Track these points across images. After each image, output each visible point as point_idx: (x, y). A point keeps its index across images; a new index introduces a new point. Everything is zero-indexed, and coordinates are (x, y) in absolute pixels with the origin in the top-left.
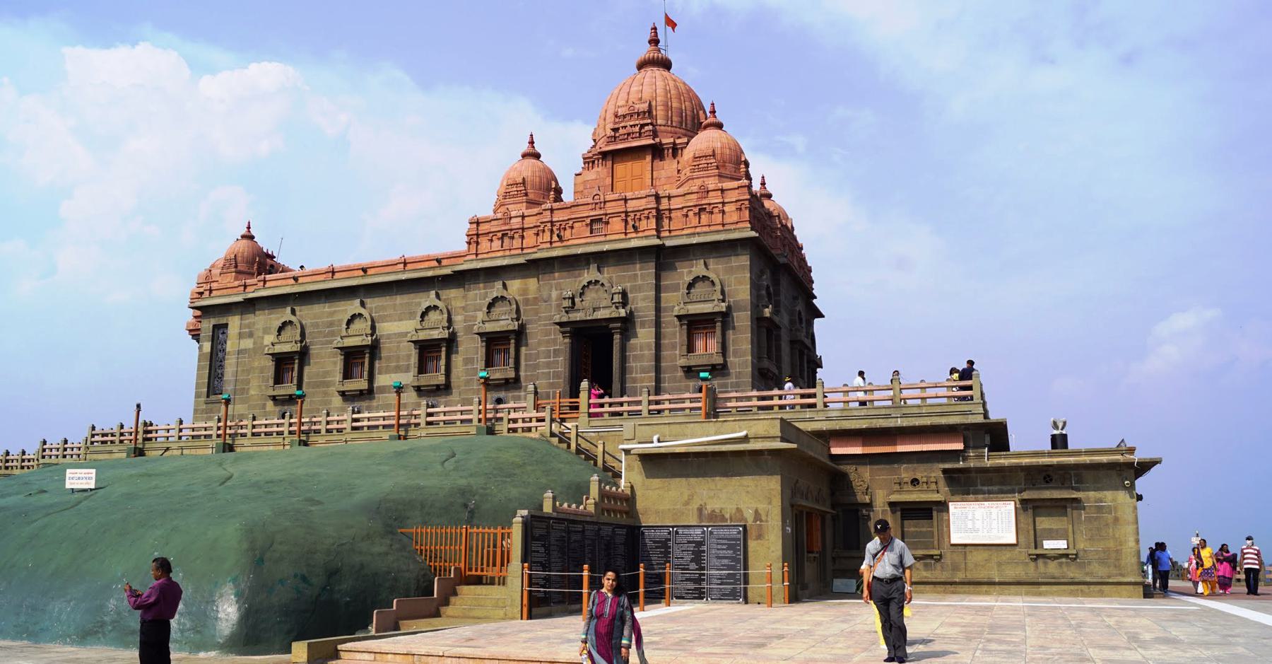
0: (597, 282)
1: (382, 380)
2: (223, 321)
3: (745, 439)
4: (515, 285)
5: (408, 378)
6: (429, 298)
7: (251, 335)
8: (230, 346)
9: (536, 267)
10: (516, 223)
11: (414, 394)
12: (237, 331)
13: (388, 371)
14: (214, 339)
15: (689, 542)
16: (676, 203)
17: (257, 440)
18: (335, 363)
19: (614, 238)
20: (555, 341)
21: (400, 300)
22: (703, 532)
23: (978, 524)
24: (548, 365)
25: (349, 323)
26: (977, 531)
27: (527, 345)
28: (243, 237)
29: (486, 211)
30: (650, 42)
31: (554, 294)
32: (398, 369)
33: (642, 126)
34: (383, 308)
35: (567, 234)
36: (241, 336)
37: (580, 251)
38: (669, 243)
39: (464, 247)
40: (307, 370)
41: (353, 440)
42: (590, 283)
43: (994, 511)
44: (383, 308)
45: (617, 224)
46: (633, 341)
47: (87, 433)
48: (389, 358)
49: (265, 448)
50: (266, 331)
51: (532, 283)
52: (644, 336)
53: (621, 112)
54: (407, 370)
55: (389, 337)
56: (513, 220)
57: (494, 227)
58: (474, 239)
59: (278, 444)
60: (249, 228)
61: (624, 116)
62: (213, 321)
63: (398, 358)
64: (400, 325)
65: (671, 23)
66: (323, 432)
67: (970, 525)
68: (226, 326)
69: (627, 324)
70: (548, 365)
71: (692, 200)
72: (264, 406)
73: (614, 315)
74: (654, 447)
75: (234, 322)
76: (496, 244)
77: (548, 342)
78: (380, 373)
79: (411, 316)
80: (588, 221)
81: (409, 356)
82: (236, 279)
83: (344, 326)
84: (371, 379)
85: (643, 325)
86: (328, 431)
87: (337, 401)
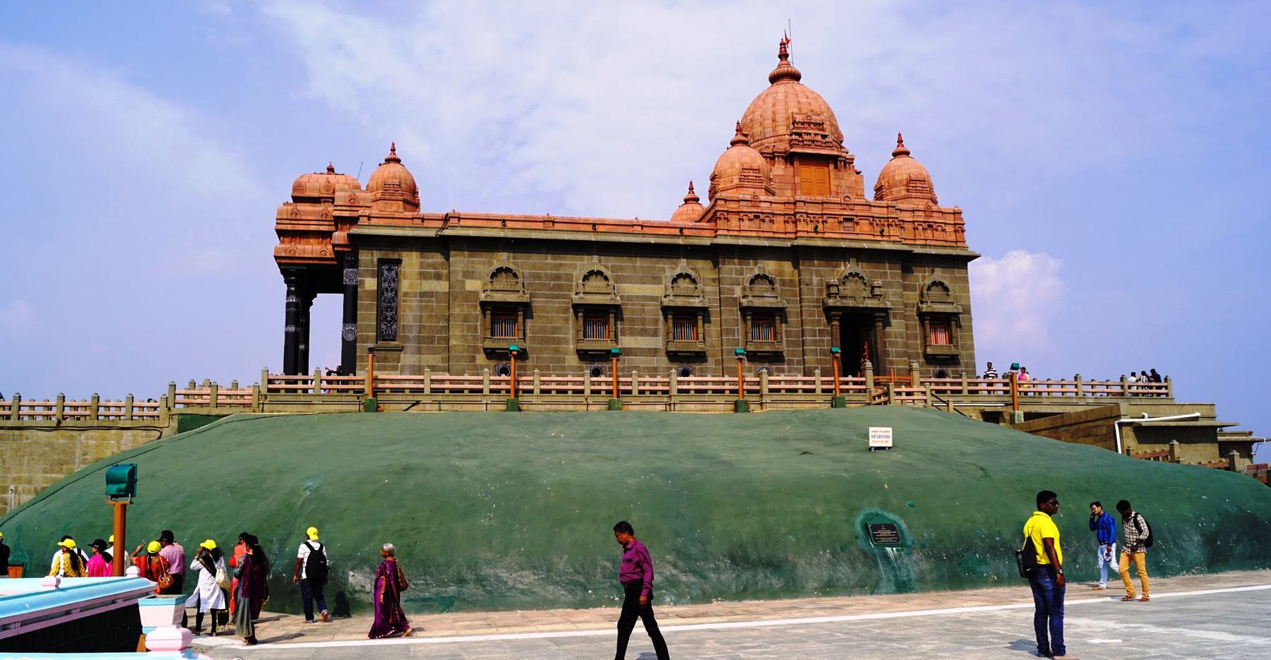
0: (857, 274)
2: (396, 257)
3: (1196, 419)
4: (770, 266)
5: (658, 342)
6: (683, 265)
7: (438, 277)
8: (405, 285)
9: (798, 255)
11: (665, 359)
12: (416, 269)
13: (631, 334)
14: (379, 275)
16: (907, 217)
17: (547, 398)
18: (566, 320)
19: (864, 237)
20: (819, 321)
21: (639, 262)
24: (815, 343)
25: (586, 278)
27: (786, 322)
28: (388, 161)
30: (780, 57)
31: (815, 279)
32: (643, 332)
34: (621, 268)
35: (820, 226)
36: (423, 276)
37: (843, 244)
38: (917, 250)
40: (529, 322)
41: (681, 403)
42: (850, 274)
44: (621, 268)
45: (864, 226)
46: (888, 329)
47: (259, 379)
48: (632, 321)
49: (563, 407)
50: (468, 274)
51: (787, 266)
52: (897, 326)
53: (799, 118)
54: (655, 334)
55: (630, 298)
56: (762, 205)
57: (744, 207)
59: (581, 403)
61: (803, 123)
62: (377, 255)
63: (643, 321)
64: (643, 288)
66: (635, 393)
68: (399, 262)
69: (883, 315)
70: (815, 343)
71: (920, 217)
72: (473, 359)
74: (1146, 421)
75: (411, 261)
77: (813, 322)
78: (623, 334)
79: (656, 280)
80: (841, 219)
81: (656, 321)
82: (405, 209)
84: (616, 341)
85: (895, 317)
87: (573, 360)
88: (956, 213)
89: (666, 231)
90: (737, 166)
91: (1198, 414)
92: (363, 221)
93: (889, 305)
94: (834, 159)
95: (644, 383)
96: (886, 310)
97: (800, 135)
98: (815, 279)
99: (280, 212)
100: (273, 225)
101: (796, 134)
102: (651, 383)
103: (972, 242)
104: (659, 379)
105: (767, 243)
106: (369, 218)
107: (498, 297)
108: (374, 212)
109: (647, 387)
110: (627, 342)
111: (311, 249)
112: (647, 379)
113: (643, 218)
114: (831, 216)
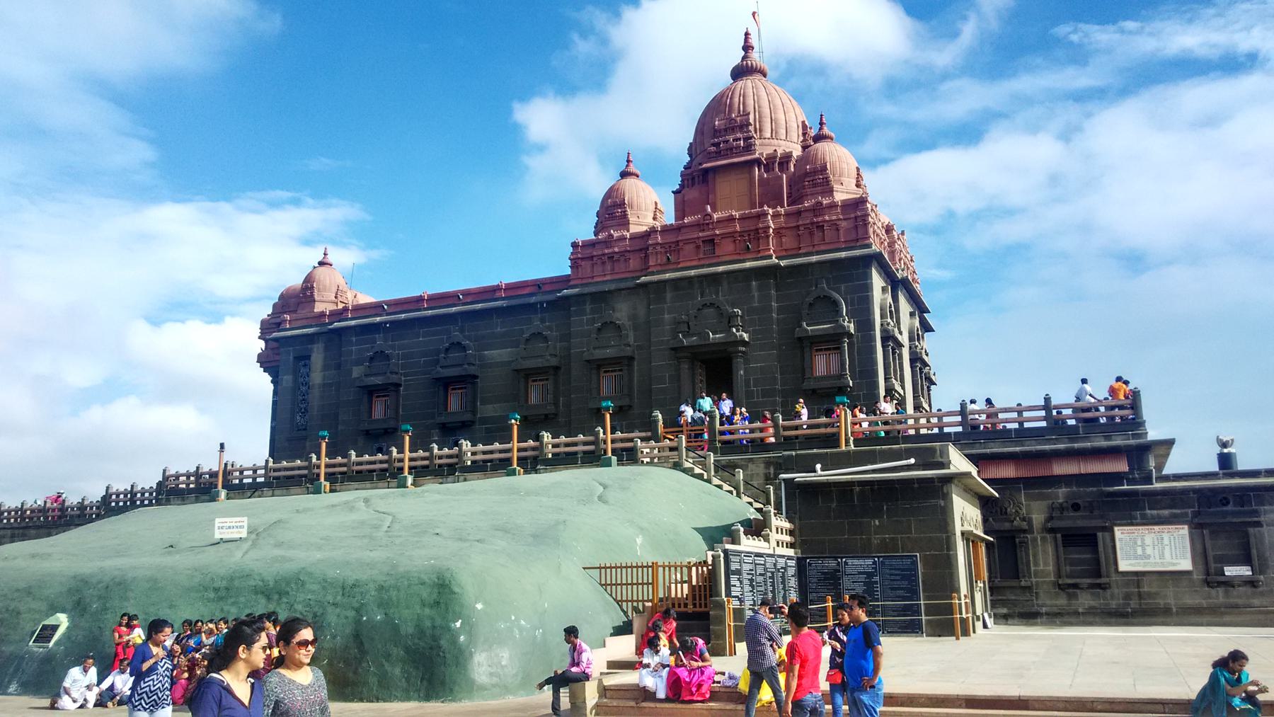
14: (296, 373)
15: (860, 573)
22: (874, 563)
23: (1149, 551)
26: (1148, 557)
29: (586, 232)
39: (568, 271)
43: (1166, 536)
58: (575, 263)
61: (726, 130)
67: (1139, 551)
68: (309, 357)
91: (912, 461)
99: (263, 322)
101: (713, 145)
114: (687, 242)
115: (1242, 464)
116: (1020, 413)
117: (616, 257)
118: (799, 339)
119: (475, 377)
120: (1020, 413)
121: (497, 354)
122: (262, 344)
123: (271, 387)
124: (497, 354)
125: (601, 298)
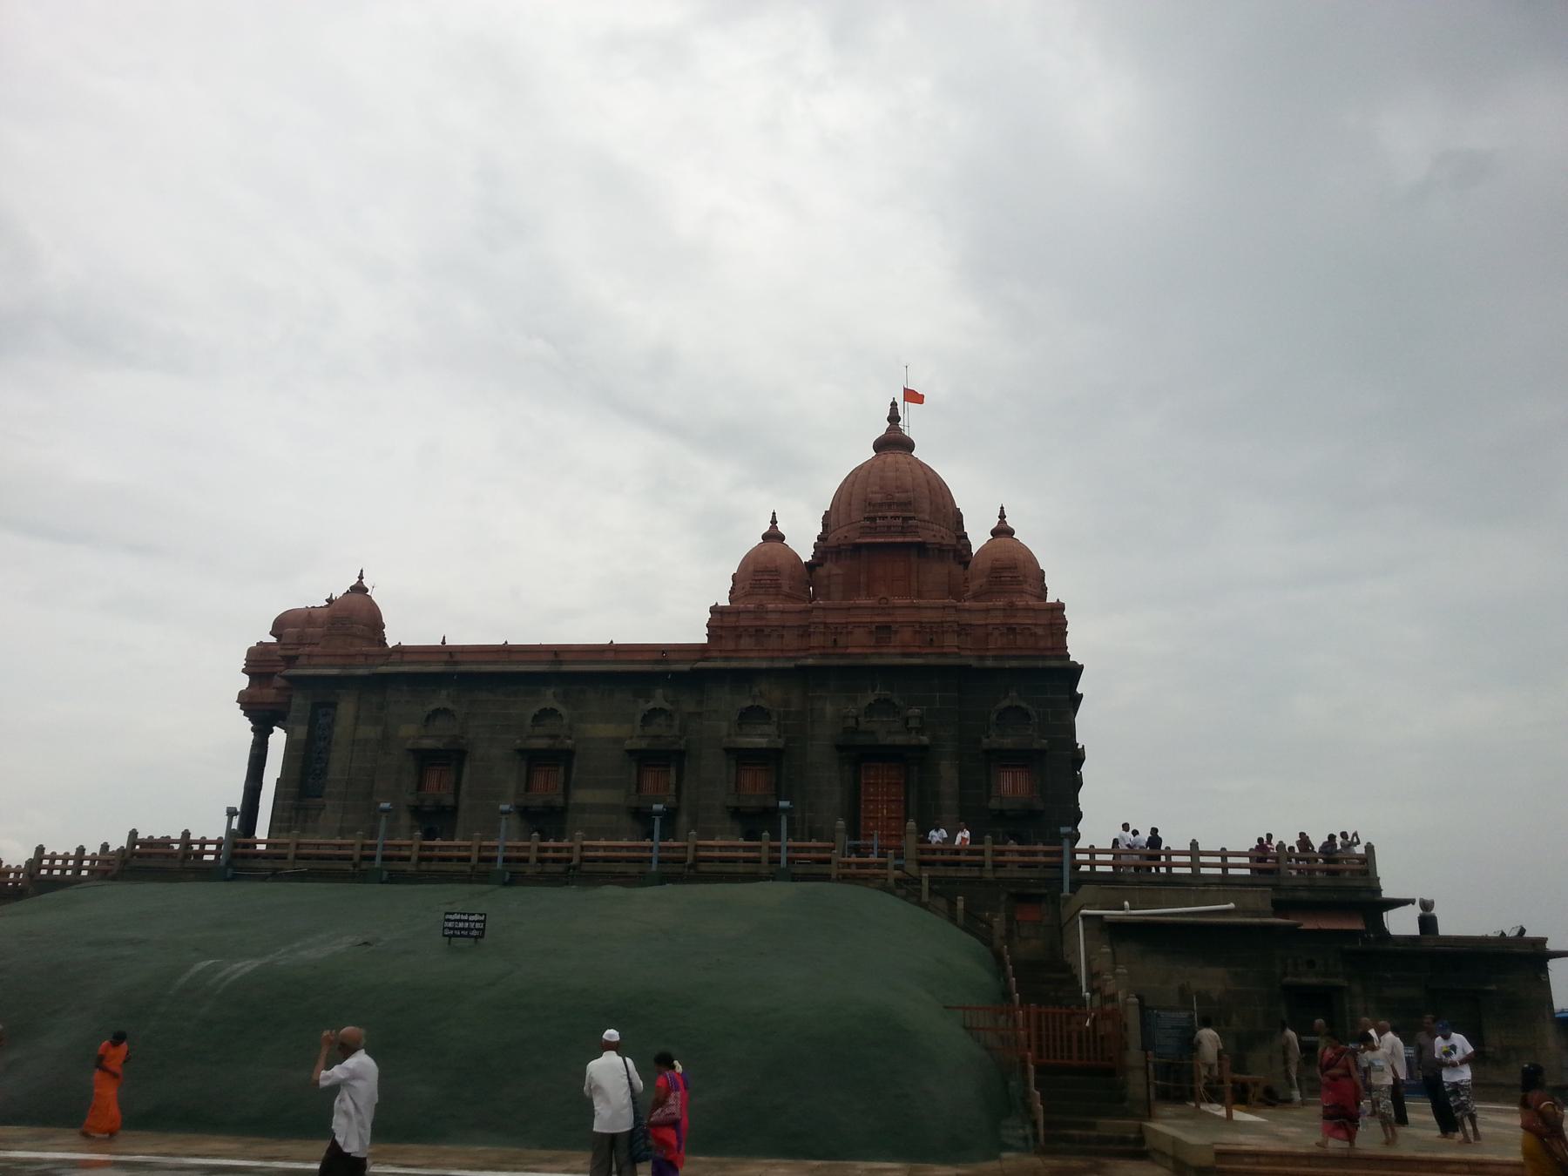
1: (581, 796)
10: (774, 619)
33: (905, 519)
39: (705, 640)
53: (878, 498)
60: (361, 577)
61: (881, 505)
65: (913, 396)
66: (533, 860)
68: (334, 706)
73: (914, 742)
76: (746, 643)
83: (529, 721)
86: (541, 861)
88: (1059, 607)
89: (647, 656)
90: (751, 568)
92: (303, 660)
93: (925, 739)
94: (922, 548)
95: (545, 849)
96: (925, 748)
97: (873, 519)
98: (829, 709)
99: (251, 651)
100: (242, 664)
102: (557, 850)
103: (1076, 653)
104: (566, 843)
105: (764, 665)
106: (309, 656)
107: (427, 743)
108: (317, 650)
109: (550, 854)
110: (581, 796)
111: (269, 694)
112: (552, 843)
113: (619, 640)
114: (859, 625)
115: (1446, 928)
116: (1092, 855)
117: (767, 631)
118: (987, 752)
119: (570, 753)
120: (1092, 855)
121: (603, 730)
122: (244, 682)
123: (251, 736)
124: (603, 730)
125: (743, 678)
